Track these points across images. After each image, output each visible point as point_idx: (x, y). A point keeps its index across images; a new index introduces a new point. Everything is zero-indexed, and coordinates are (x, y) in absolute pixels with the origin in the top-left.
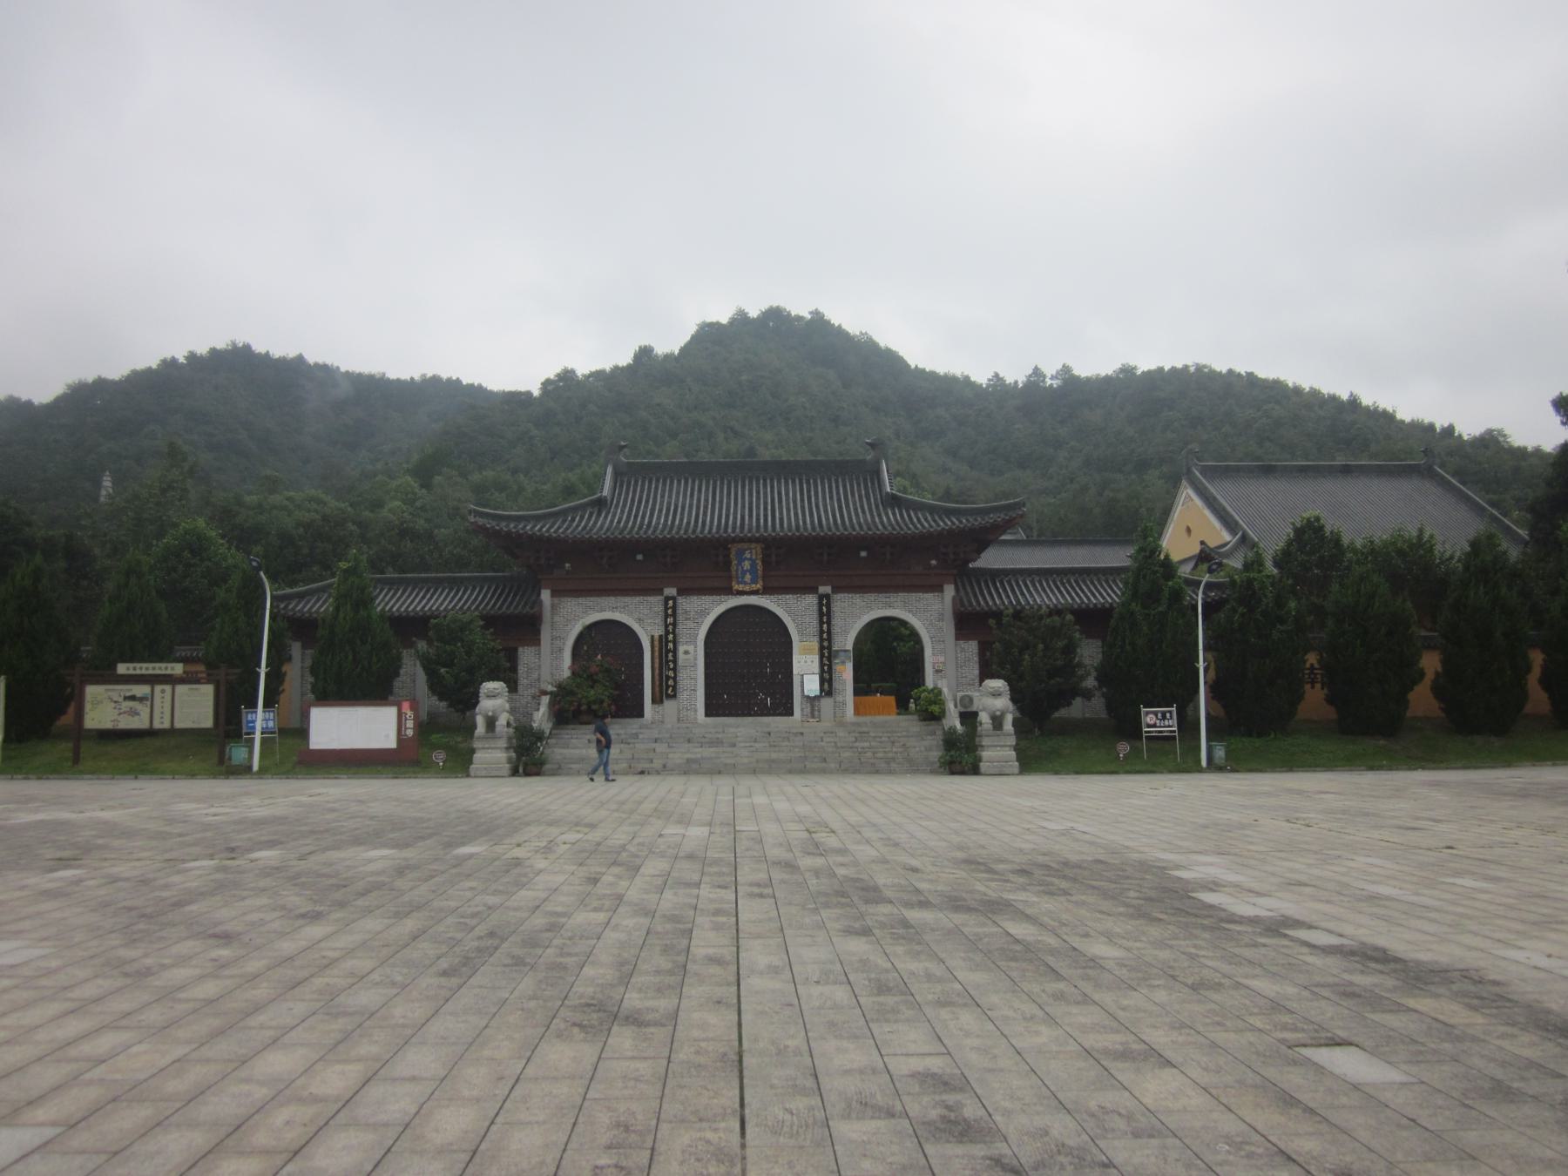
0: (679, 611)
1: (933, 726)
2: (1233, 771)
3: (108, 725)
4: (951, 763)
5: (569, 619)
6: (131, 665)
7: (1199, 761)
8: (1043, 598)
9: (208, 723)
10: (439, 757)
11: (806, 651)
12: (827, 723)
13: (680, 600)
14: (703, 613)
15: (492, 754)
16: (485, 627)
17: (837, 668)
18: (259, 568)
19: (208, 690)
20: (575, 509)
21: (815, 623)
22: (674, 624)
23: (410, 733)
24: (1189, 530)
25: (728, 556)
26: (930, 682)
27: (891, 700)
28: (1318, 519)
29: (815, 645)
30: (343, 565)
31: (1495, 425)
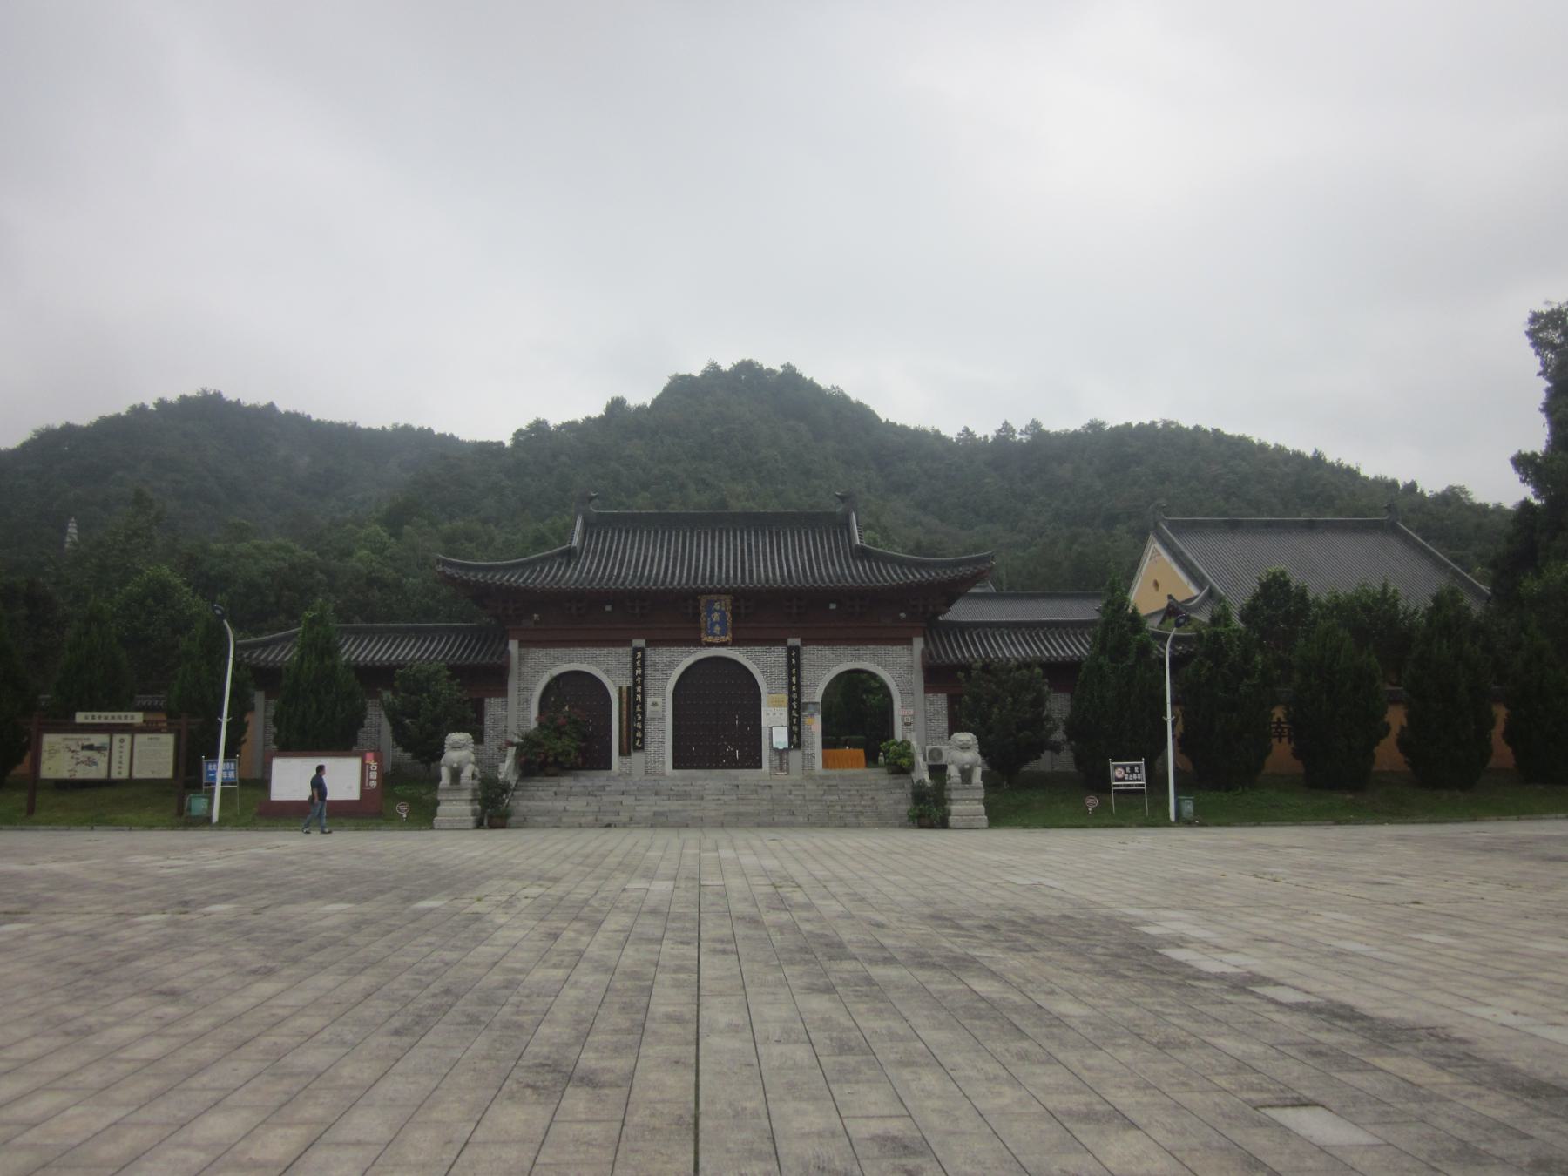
0: (648, 663)
1: (902, 780)
2: (1202, 825)
3: (65, 775)
4: (920, 816)
5: (537, 669)
6: (90, 714)
7: (1168, 814)
8: (1011, 651)
9: (168, 773)
10: (403, 809)
11: (775, 704)
12: (796, 776)
13: (649, 651)
15: (456, 807)
16: (451, 678)
17: (806, 720)
18: (222, 617)
19: (168, 740)
20: (543, 560)
21: (784, 676)
22: (643, 676)
23: (374, 784)
24: (1156, 584)
25: (697, 607)
26: (899, 734)
27: (861, 752)
28: (1283, 574)
29: (785, 698)
30: (309, 614)
31: (1456, 483)
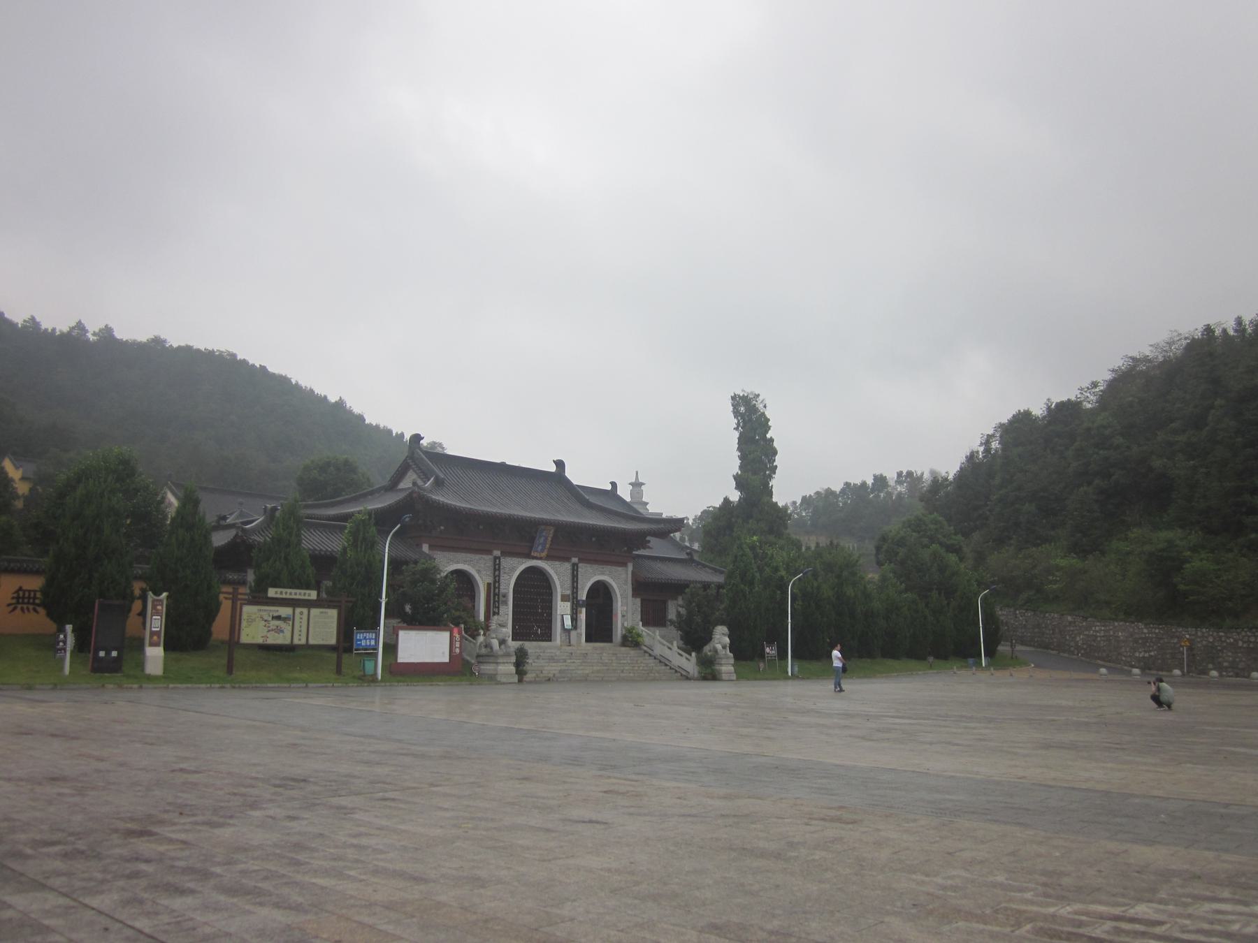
2: (803, 678)
3: (260, 641)
6: (279, 590)
9: (333, 641)
14: (515, 568)
18: (982, 584)
19: (333, 613)
31: (437, 440)
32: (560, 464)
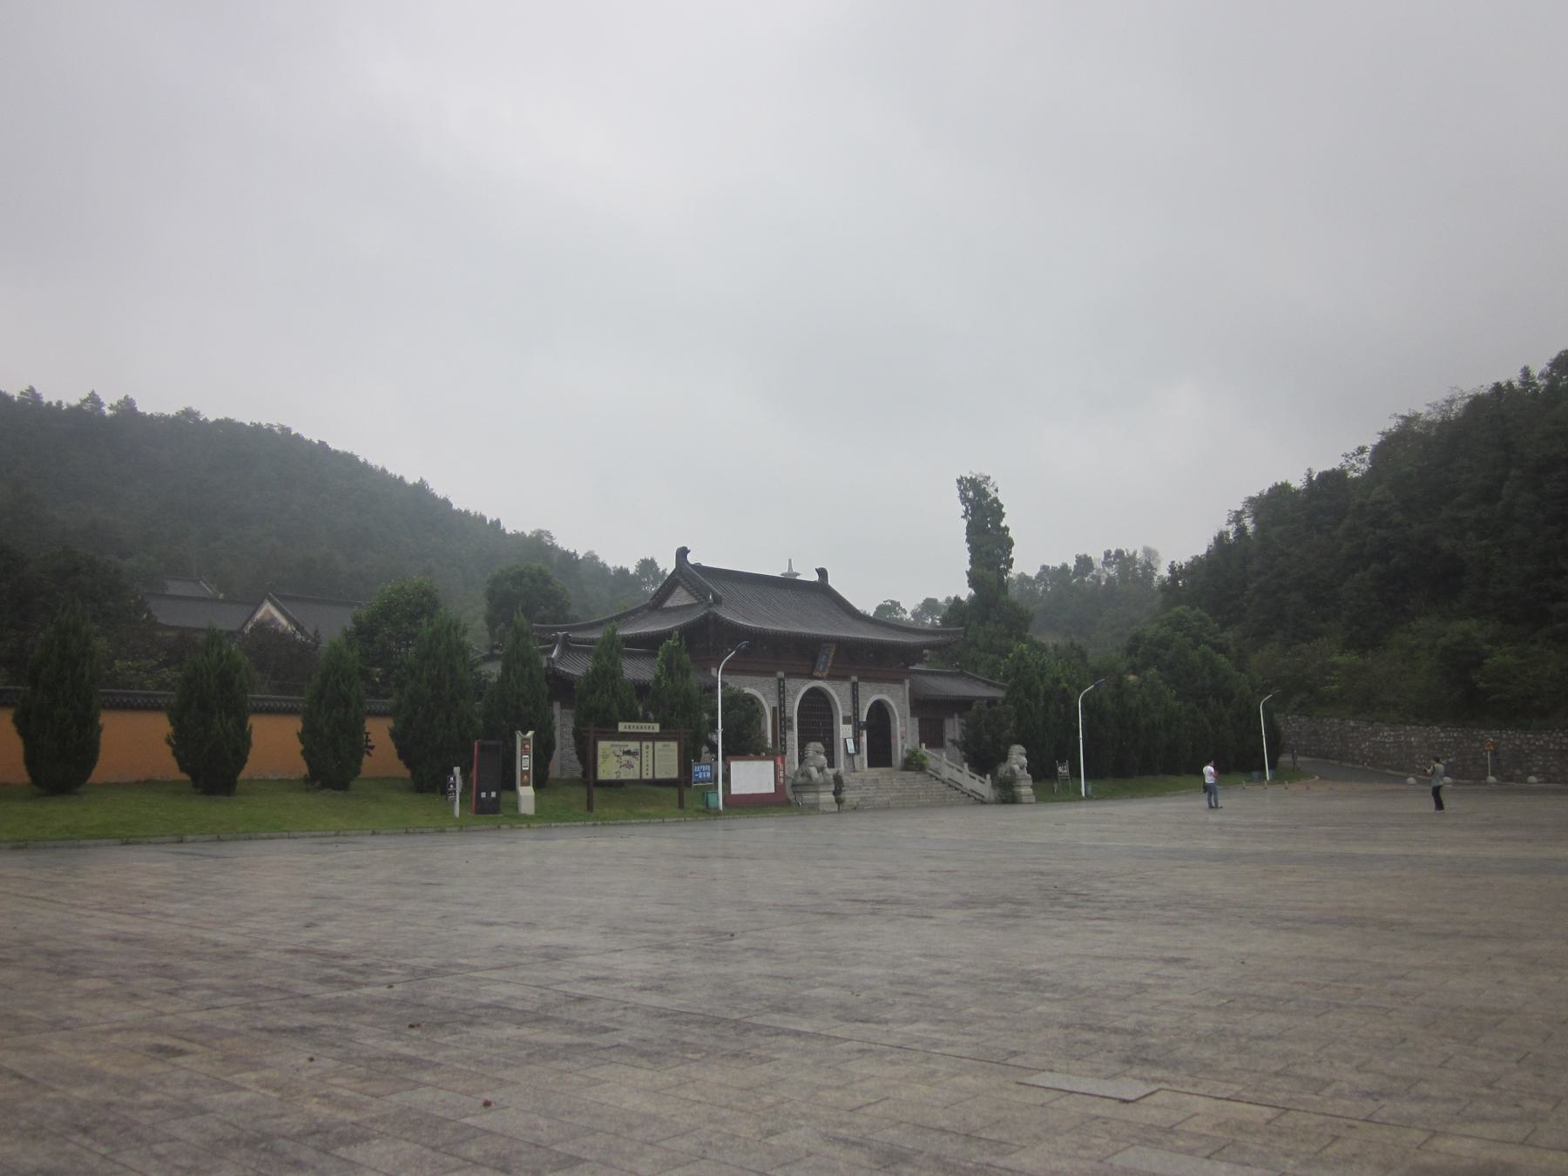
3: (614, 777)
9: (675, 775)
14: (799, 689)
19: (674, 745)
32: (822, 573)
